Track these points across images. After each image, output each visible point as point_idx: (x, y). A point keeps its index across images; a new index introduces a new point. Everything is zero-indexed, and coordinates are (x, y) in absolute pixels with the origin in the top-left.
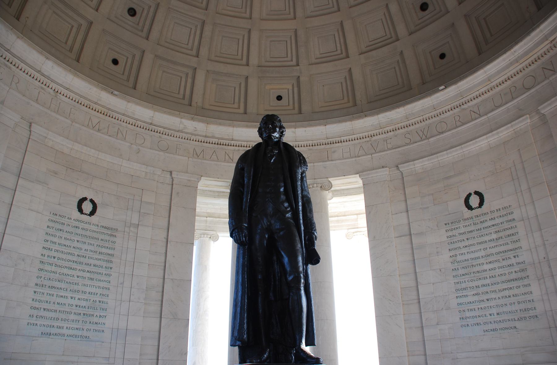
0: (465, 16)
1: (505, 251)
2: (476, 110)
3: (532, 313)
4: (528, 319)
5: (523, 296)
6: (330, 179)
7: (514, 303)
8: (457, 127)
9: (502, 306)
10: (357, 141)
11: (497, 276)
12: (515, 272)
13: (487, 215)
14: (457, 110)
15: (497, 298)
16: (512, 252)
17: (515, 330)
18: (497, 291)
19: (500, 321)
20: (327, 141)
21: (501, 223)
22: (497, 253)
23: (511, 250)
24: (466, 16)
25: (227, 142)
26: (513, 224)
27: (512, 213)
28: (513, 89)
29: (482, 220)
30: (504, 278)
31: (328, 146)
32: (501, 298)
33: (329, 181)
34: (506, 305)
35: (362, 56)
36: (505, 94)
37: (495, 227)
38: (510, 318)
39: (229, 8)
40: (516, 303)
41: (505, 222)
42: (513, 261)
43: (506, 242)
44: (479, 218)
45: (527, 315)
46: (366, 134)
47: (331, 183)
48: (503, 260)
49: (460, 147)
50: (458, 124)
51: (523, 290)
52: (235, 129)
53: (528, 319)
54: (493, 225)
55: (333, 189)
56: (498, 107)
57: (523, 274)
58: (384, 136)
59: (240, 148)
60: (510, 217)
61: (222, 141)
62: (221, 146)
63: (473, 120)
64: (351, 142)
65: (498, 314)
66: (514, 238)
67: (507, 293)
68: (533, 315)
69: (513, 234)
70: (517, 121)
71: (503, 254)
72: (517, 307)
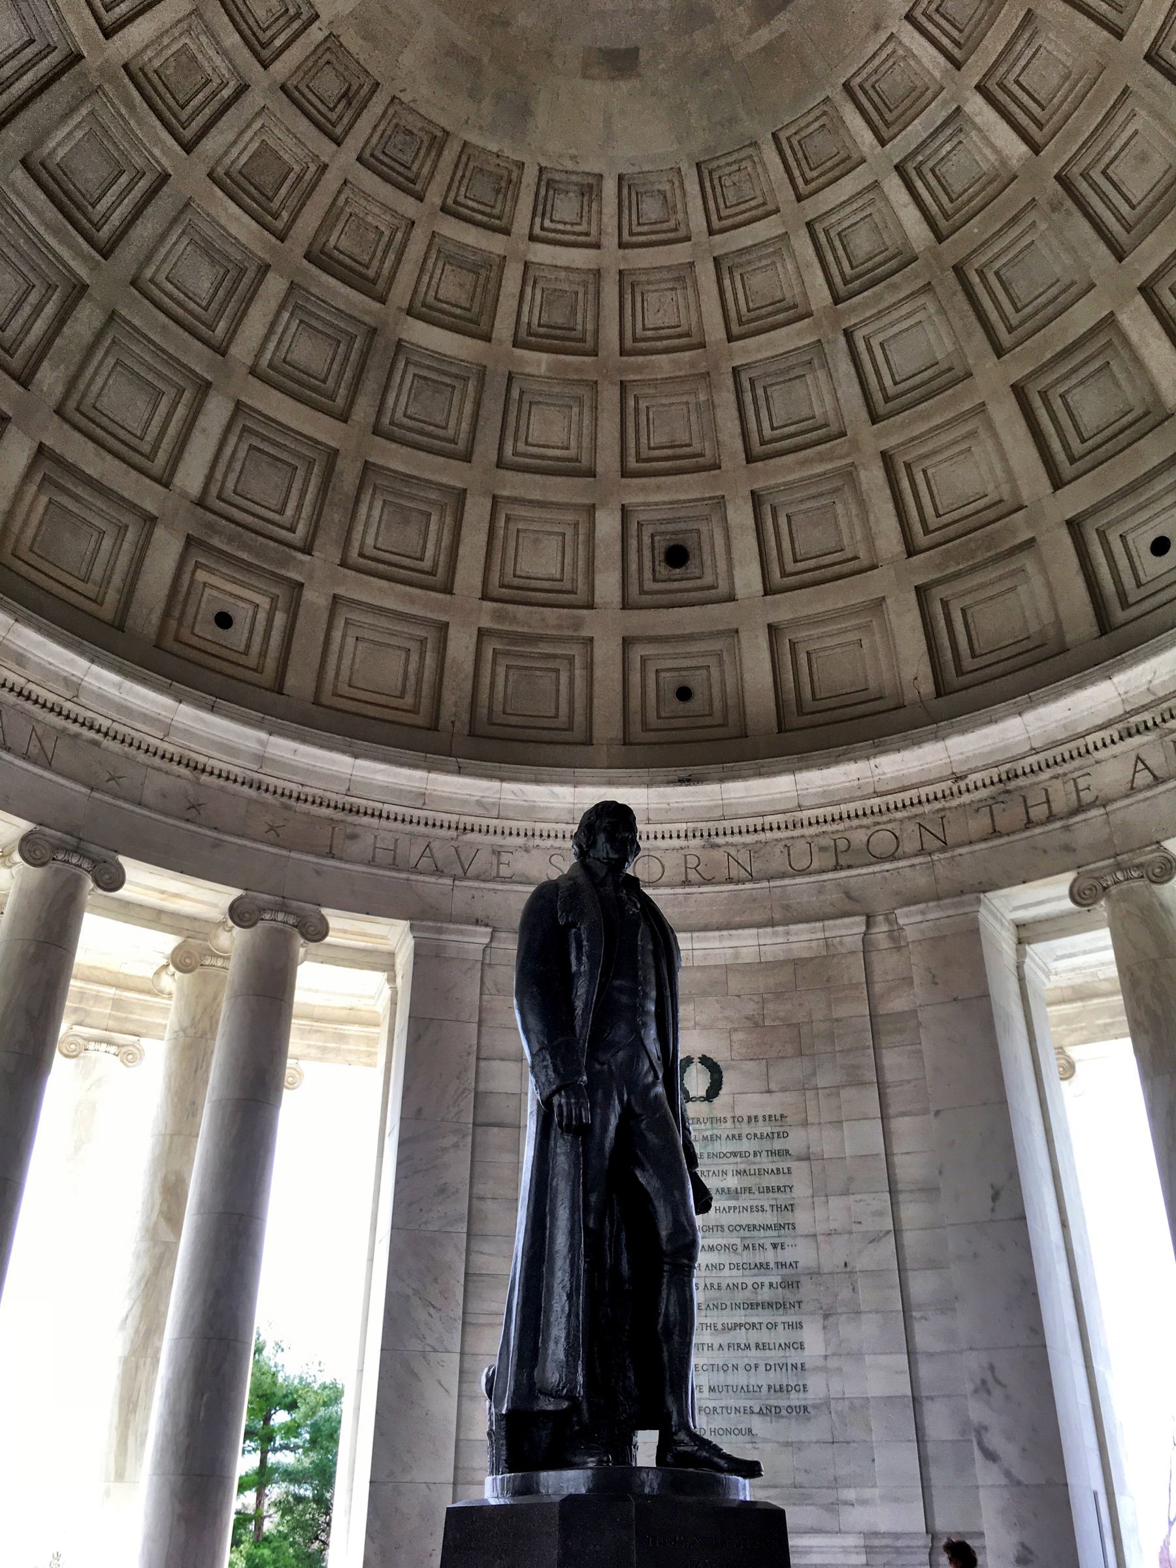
0: (770, 626)
1: (754, 1227)
2: (743, 857)
3: (795, 1399)
4: (784, 1412)
5: (781, 1353)
6: (325, 911)
7: (756, 1366)
8: (686, 883)
9: (725, 1368)
10: (422, 829)
11: (724, 1285)
12: (771, 1285)
13: (723, 1125)
14: (698, 842)
15: (716, 1346)
16: (769, 1233)
17: (747, 1438)
18: (719, 1327)
19: (715, 1409)
20: (341, 800)
21: (755, 1153)
22: (733, 1228)
23: (769, 1227)
24: (773, 630)
25: (52, 698)
26: (783, 1165)
27: (785, 1135)
28: (842, 844)
29: (708, 1133)
30: (740, 1296)
31: (339, 815)
32: (726, 1348)
33: (322, 916)
34: (735, 1367)
35: (487, 604)
36: (822, 849)
37: (738, 1159)
38: (742, 1403)
39: (169, 287)
40: (762, 1368)
41: (764, 1154)
42: (770, 1256)
43: (760, 1203)
44: (703, 1126)
45: (783, 1403)
46: (454, 818)
47: (327, 924)
48: (746, 1248)
49: (689, 935)
50: (693, 876)
51: (782, 1336)
52: (95, 668)
53: (784, 1412)
54: (734, 1154)
55: (328, 939)
56: (802, 873)
57: (790, 1296)
58: (498, 840)
59: (84, 731)
60: (778, 1145)
61: (36, 690)
62: (28, 705)
63: (730, 880)
64: (408, 828)
65: (712, 1389)
66: (782, 1199)
67: (741, 1336)
68: (797, 1403)
69: (779, 1188)
70: (839, 922)
71: (747, 1234)
72: (762, 1379)
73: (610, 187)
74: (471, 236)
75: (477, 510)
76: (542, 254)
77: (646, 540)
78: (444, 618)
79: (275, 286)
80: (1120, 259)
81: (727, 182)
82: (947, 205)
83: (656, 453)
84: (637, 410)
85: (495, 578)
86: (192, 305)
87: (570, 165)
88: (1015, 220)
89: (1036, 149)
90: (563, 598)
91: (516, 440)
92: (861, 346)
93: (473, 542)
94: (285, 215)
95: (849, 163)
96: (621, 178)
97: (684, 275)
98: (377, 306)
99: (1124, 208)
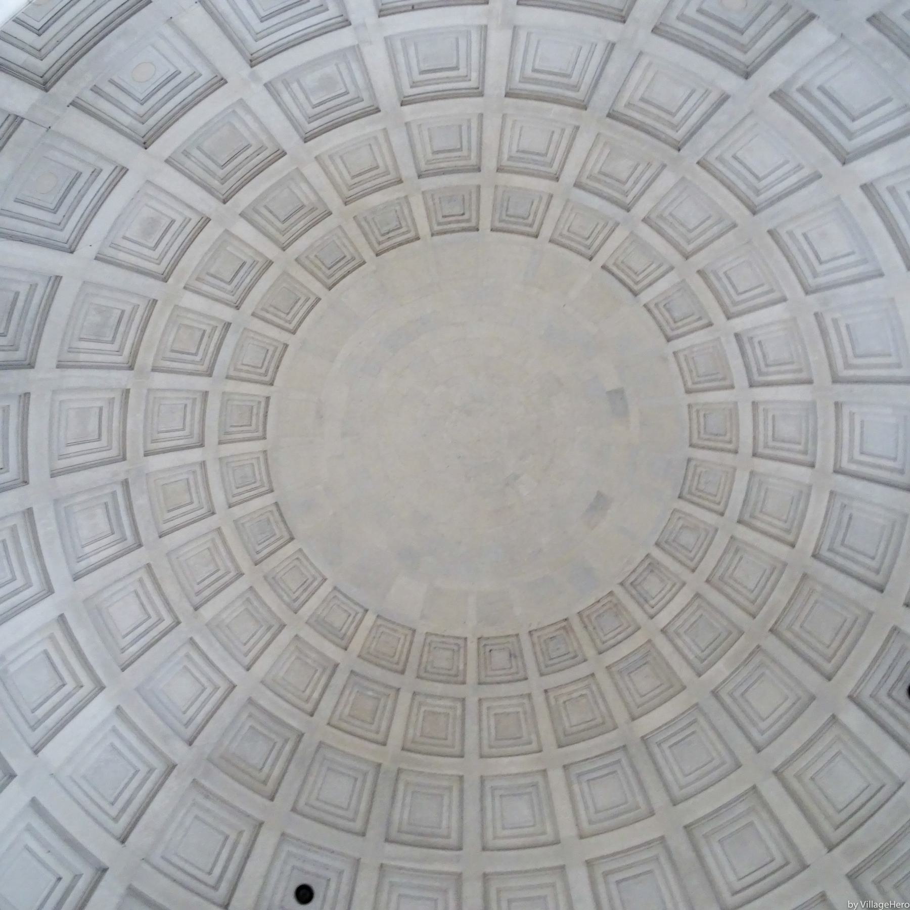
35: (837, 852)
73: (657, 554)
74: (625, 649)
75: (772, 791)
76: (663, 618)
77: (889, 702)
78: (817, 890)
79: (556, 777)
80: (881, 275)
81: (702, 487)
82: (794, 367)
83: (835, 645)
84: (798, 636)
85: (827, 827)
86: (526, 831)
87: (631, 568)
88: (824, 333)
89: (784, 299)
90: (881, 796)
91: (755, 725)
92: (853, 467)
93: (789, 814)
94: (533, 737)
95: (733, 412)
96: (657, 544)
97: (734, 546)
98: (614, 734)
99: (852, 259)
